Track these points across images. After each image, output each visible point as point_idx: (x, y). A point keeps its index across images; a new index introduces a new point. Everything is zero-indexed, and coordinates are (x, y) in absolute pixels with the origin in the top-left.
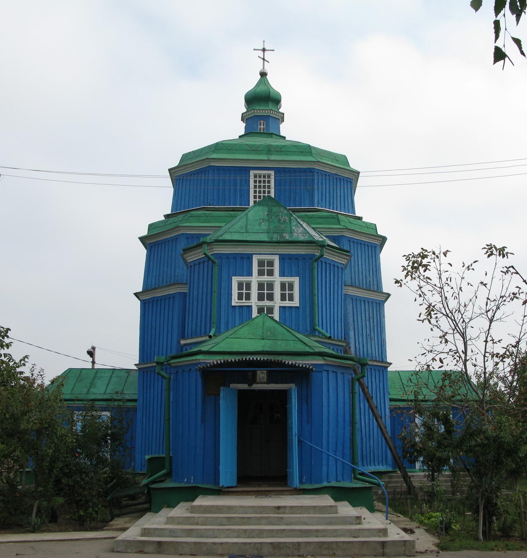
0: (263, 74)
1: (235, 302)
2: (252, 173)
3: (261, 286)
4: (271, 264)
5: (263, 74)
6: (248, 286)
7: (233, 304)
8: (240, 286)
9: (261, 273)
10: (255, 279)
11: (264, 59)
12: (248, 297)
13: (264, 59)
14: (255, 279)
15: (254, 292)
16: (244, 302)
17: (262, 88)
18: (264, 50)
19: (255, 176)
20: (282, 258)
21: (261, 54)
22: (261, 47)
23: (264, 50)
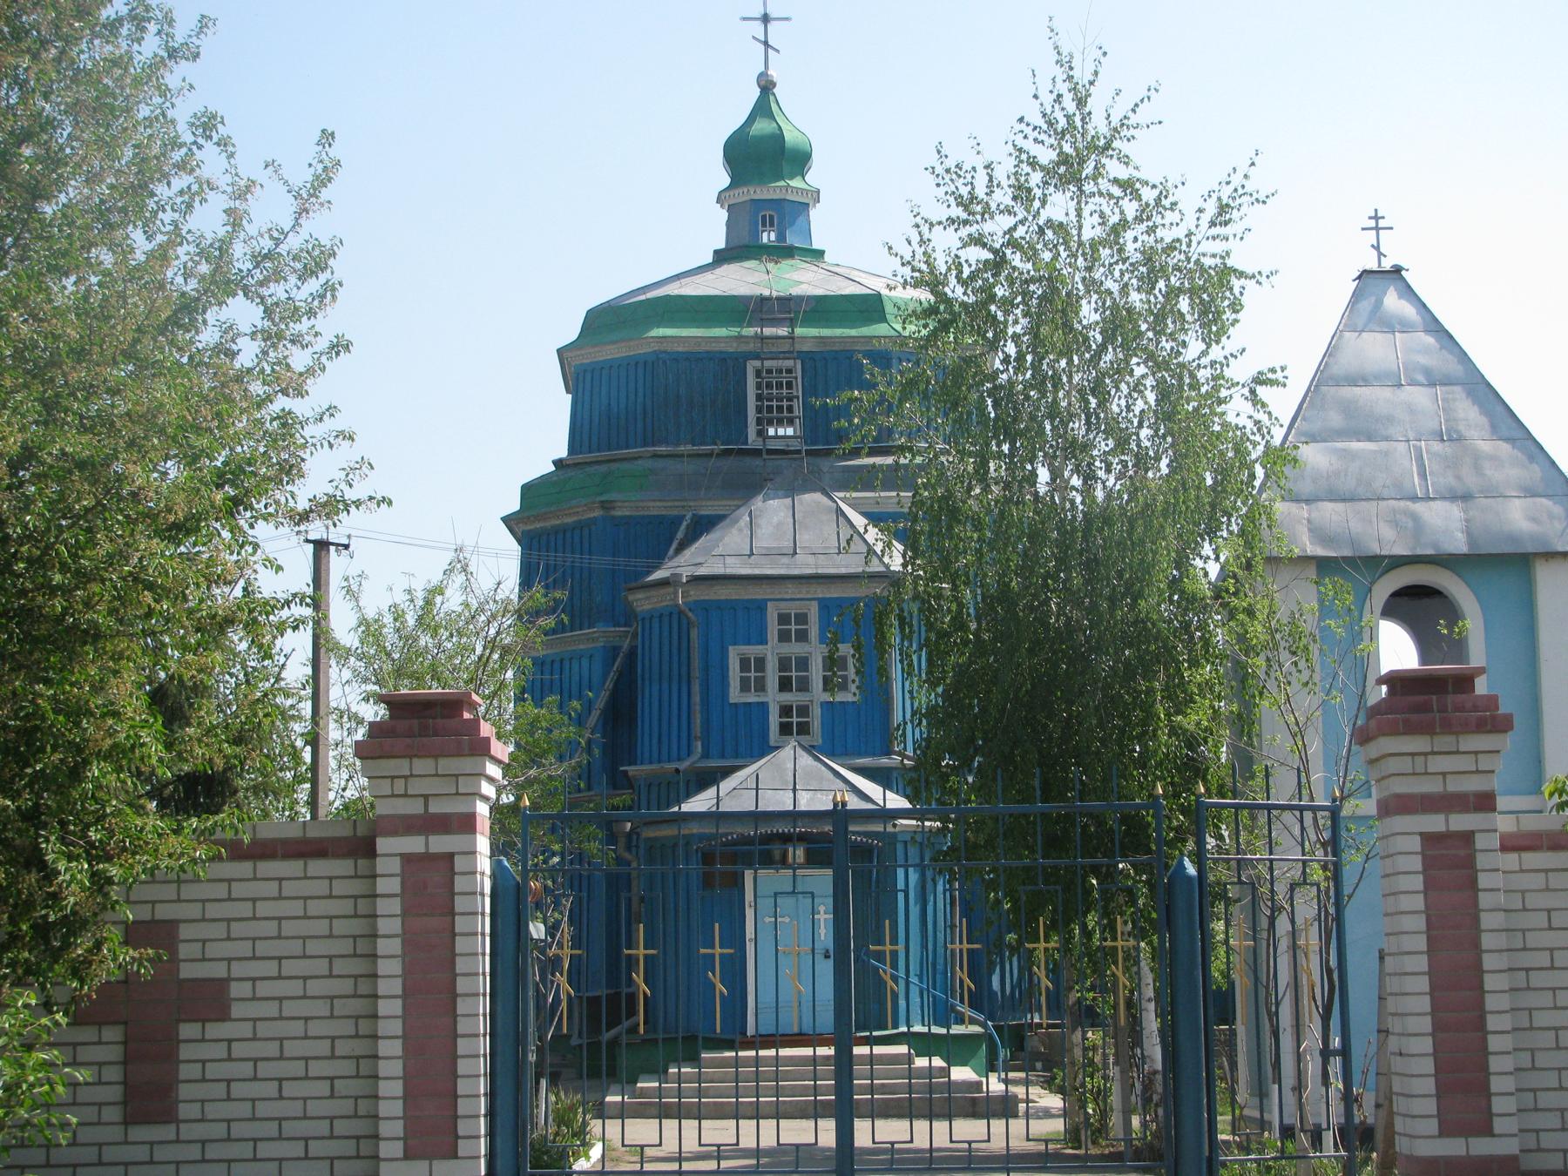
0: (766, 86)
1: (735, 695)
2: (752, 365)
3: (784, 664)
4: (802, 618)
5: (766, 86)
6: (761, 663)
7: (732, 701)
8: (745, 664)
9: (784, 637)
10: (771, 651)
11: (766, 43)
12: (761, 686)
13: (766, 43)
14: (771, 651)
15: (772, 677)
16: (752, 698)
17: (761, 127)
18: (766, 19)
19: (758, 373)
20: (825, 605)
21: (758, 29)
22: (758, 12)
23: (766, 19)
